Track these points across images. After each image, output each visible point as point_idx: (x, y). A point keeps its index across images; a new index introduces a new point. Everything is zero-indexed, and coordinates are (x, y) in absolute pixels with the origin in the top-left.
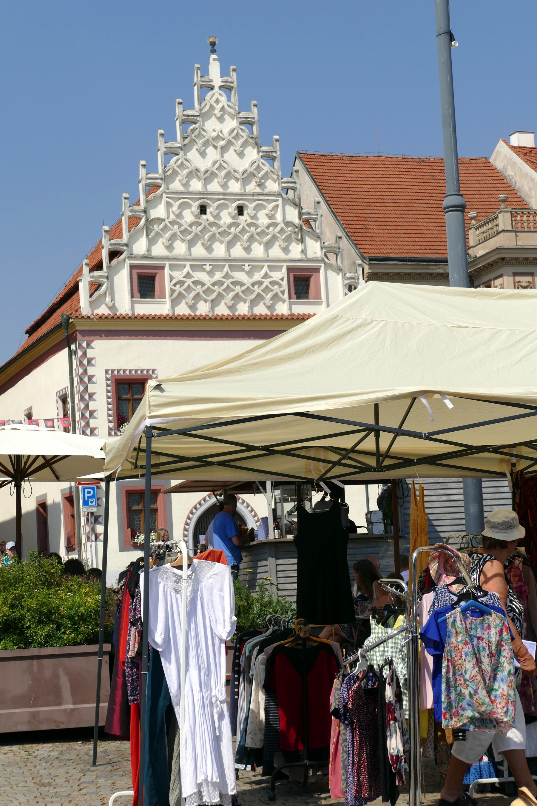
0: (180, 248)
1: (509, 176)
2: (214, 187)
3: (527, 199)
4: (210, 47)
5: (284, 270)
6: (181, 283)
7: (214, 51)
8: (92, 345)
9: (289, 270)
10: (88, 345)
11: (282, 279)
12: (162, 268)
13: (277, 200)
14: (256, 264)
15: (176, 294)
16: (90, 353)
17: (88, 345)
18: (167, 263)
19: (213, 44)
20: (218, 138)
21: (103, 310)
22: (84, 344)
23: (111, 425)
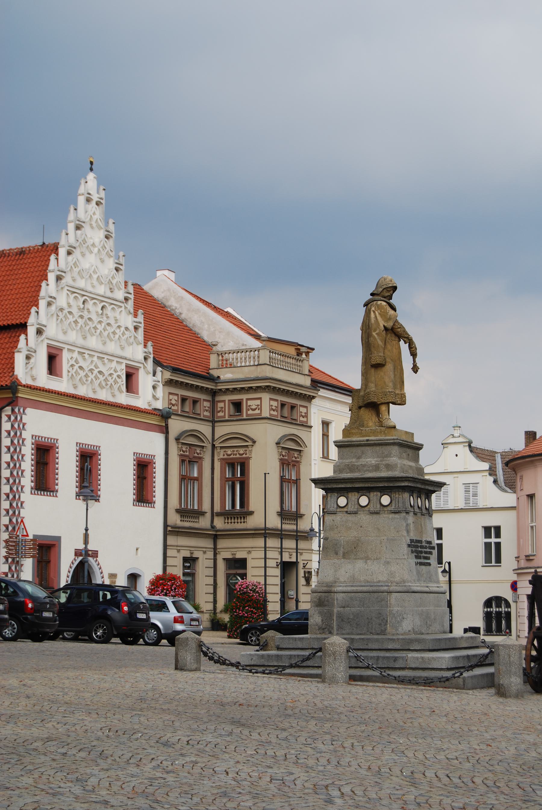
0: (73, 336)
1: (170, 307)
3: (196, 330)
4: (90, 165)
5: (123, 367)
6: (72, 366)
7: (91, 169)
8: (26, 411)
10: (24, 411)
11: (122, 374)
12: (61, 350)
13: (121, 307)
15: (70, 374)
17: (24, 411)
18: (67, 347)
20: (93, 245)
21: (30, 382)
22: (22, 410)
23: (33, 484)
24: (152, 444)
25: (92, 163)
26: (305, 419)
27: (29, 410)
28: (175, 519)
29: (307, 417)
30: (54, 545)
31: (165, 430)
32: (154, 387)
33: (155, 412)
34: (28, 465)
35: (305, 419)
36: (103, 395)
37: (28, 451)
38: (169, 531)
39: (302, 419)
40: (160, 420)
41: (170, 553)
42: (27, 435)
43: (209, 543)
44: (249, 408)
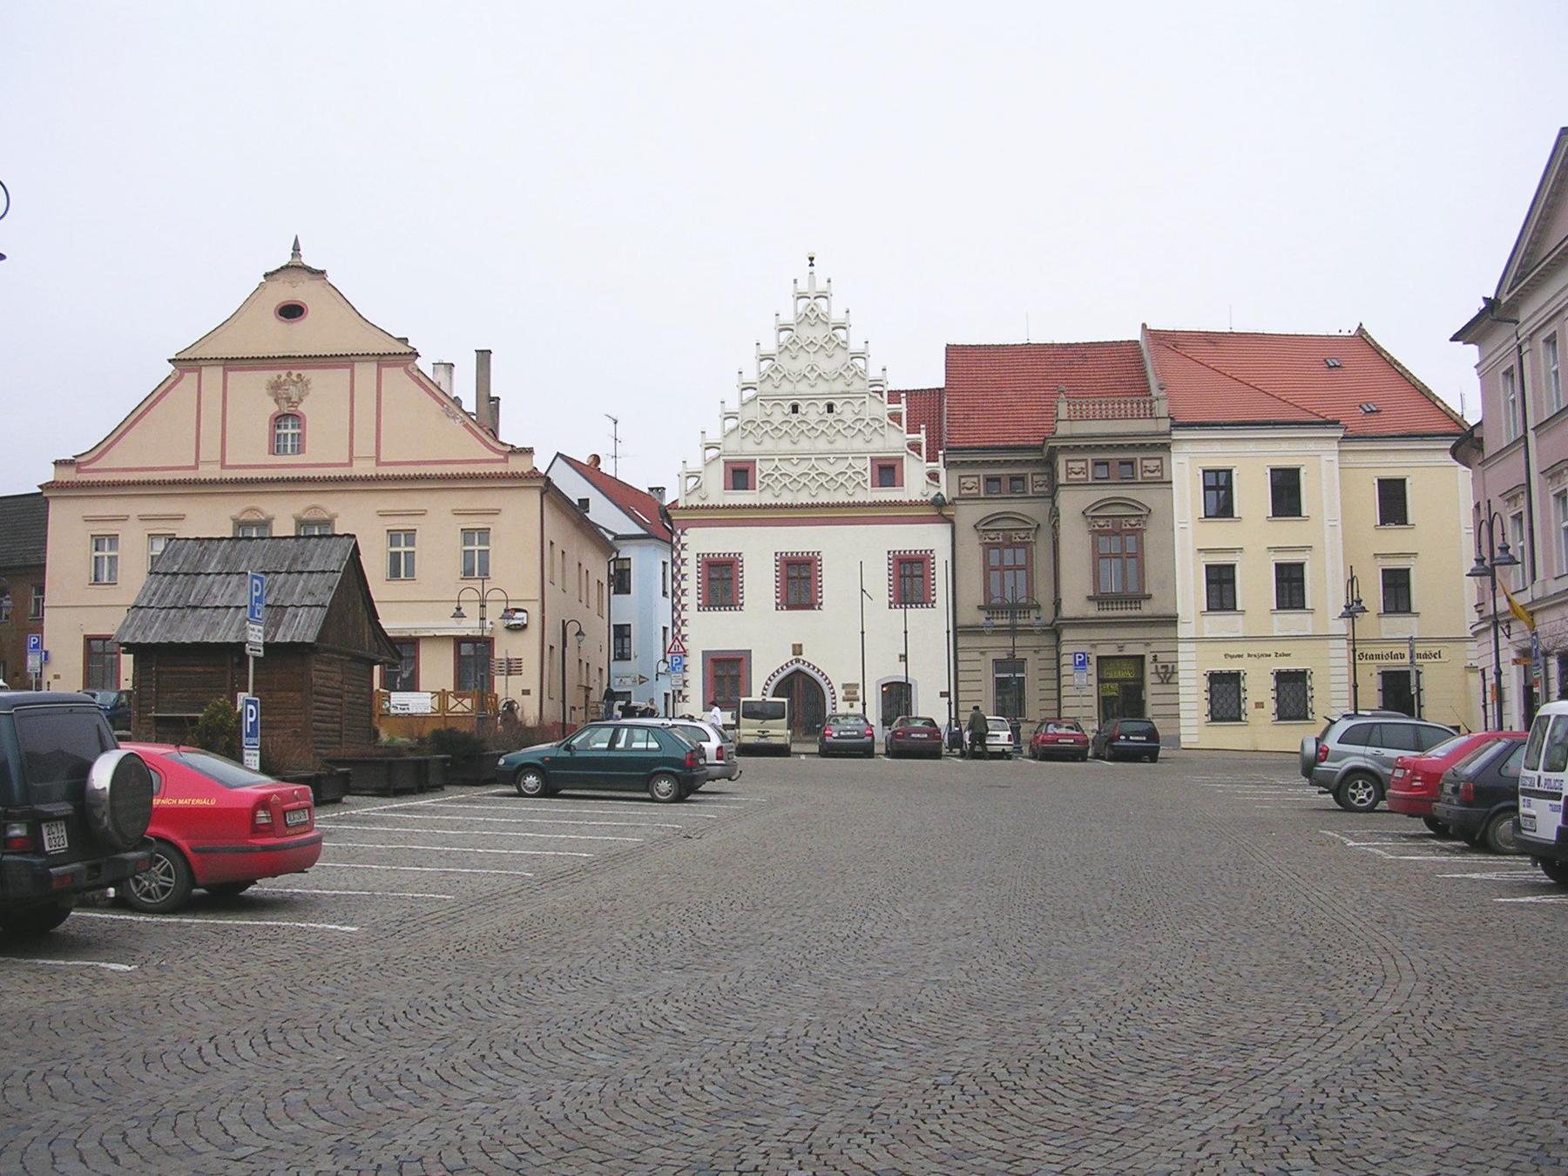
0: (768, 445)
2: (803, 387)
9: (872, 459)
14: (841, 456)
16: (683, 539)
19: (811, 259)
24: (932, 539)
25: (811, 259)
26: (1158, 474)
27: (689, 531)
28: (971, 616)
29: (1162, 471)
30: (740, 660)
31: (949, 520)
32: (934, 476)
33: (938, 503)
34: (692, 584)
35: (1158, 474)
36: (860, 497)
37: (691, 570)
38: (959, 631)
39: (1147, 474)
40: (938, 511)
41: (961, 656)
42: (690, 555)
43: (1048, 640)
44: (1145, 469)
